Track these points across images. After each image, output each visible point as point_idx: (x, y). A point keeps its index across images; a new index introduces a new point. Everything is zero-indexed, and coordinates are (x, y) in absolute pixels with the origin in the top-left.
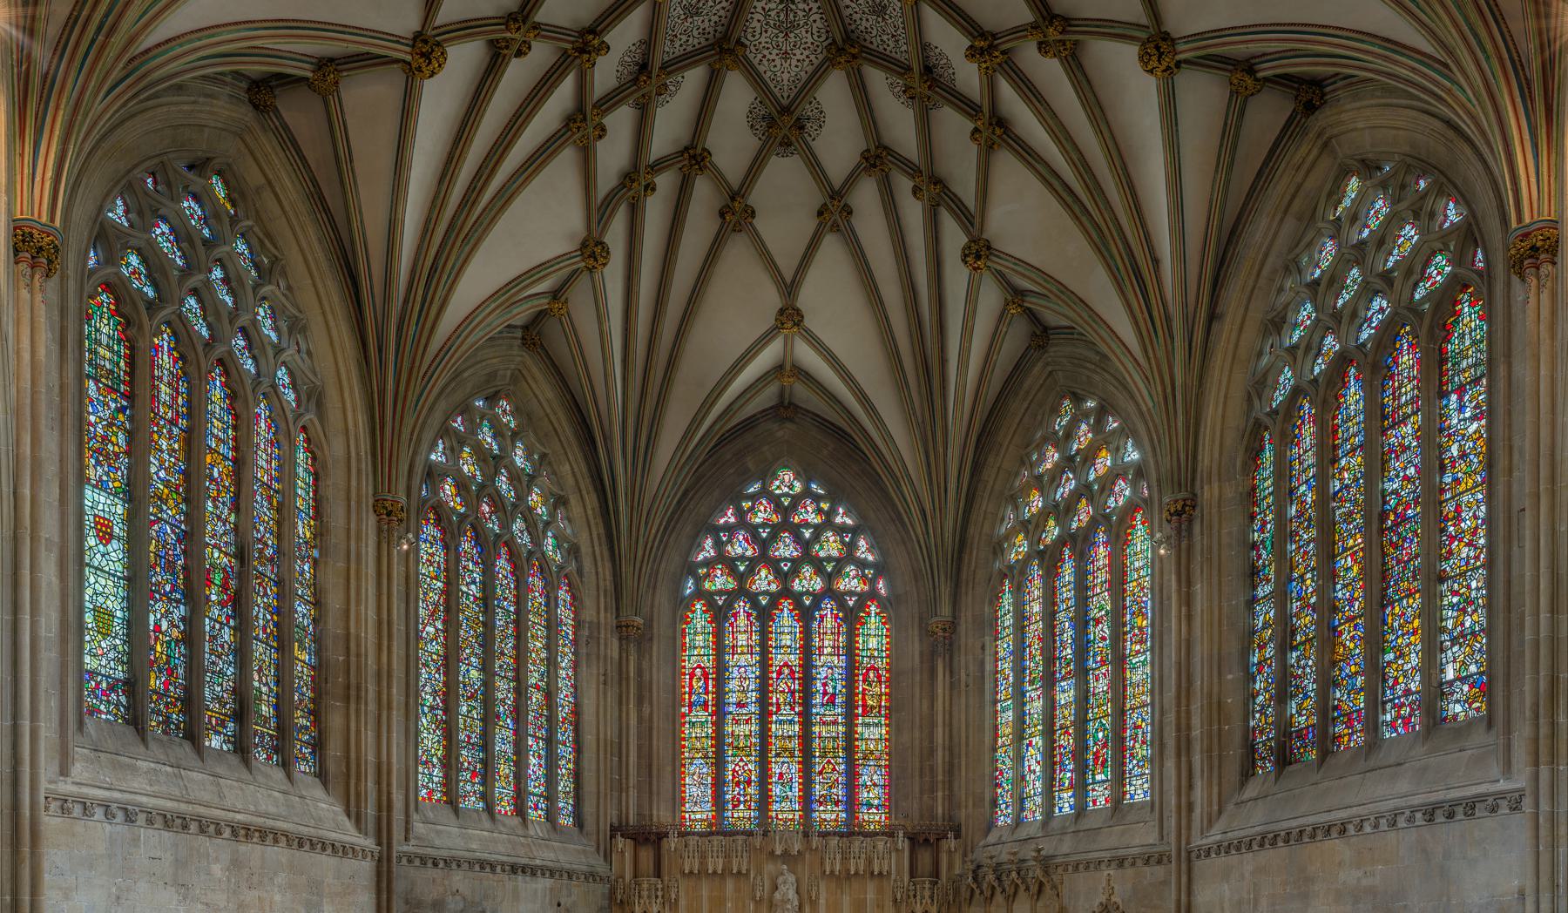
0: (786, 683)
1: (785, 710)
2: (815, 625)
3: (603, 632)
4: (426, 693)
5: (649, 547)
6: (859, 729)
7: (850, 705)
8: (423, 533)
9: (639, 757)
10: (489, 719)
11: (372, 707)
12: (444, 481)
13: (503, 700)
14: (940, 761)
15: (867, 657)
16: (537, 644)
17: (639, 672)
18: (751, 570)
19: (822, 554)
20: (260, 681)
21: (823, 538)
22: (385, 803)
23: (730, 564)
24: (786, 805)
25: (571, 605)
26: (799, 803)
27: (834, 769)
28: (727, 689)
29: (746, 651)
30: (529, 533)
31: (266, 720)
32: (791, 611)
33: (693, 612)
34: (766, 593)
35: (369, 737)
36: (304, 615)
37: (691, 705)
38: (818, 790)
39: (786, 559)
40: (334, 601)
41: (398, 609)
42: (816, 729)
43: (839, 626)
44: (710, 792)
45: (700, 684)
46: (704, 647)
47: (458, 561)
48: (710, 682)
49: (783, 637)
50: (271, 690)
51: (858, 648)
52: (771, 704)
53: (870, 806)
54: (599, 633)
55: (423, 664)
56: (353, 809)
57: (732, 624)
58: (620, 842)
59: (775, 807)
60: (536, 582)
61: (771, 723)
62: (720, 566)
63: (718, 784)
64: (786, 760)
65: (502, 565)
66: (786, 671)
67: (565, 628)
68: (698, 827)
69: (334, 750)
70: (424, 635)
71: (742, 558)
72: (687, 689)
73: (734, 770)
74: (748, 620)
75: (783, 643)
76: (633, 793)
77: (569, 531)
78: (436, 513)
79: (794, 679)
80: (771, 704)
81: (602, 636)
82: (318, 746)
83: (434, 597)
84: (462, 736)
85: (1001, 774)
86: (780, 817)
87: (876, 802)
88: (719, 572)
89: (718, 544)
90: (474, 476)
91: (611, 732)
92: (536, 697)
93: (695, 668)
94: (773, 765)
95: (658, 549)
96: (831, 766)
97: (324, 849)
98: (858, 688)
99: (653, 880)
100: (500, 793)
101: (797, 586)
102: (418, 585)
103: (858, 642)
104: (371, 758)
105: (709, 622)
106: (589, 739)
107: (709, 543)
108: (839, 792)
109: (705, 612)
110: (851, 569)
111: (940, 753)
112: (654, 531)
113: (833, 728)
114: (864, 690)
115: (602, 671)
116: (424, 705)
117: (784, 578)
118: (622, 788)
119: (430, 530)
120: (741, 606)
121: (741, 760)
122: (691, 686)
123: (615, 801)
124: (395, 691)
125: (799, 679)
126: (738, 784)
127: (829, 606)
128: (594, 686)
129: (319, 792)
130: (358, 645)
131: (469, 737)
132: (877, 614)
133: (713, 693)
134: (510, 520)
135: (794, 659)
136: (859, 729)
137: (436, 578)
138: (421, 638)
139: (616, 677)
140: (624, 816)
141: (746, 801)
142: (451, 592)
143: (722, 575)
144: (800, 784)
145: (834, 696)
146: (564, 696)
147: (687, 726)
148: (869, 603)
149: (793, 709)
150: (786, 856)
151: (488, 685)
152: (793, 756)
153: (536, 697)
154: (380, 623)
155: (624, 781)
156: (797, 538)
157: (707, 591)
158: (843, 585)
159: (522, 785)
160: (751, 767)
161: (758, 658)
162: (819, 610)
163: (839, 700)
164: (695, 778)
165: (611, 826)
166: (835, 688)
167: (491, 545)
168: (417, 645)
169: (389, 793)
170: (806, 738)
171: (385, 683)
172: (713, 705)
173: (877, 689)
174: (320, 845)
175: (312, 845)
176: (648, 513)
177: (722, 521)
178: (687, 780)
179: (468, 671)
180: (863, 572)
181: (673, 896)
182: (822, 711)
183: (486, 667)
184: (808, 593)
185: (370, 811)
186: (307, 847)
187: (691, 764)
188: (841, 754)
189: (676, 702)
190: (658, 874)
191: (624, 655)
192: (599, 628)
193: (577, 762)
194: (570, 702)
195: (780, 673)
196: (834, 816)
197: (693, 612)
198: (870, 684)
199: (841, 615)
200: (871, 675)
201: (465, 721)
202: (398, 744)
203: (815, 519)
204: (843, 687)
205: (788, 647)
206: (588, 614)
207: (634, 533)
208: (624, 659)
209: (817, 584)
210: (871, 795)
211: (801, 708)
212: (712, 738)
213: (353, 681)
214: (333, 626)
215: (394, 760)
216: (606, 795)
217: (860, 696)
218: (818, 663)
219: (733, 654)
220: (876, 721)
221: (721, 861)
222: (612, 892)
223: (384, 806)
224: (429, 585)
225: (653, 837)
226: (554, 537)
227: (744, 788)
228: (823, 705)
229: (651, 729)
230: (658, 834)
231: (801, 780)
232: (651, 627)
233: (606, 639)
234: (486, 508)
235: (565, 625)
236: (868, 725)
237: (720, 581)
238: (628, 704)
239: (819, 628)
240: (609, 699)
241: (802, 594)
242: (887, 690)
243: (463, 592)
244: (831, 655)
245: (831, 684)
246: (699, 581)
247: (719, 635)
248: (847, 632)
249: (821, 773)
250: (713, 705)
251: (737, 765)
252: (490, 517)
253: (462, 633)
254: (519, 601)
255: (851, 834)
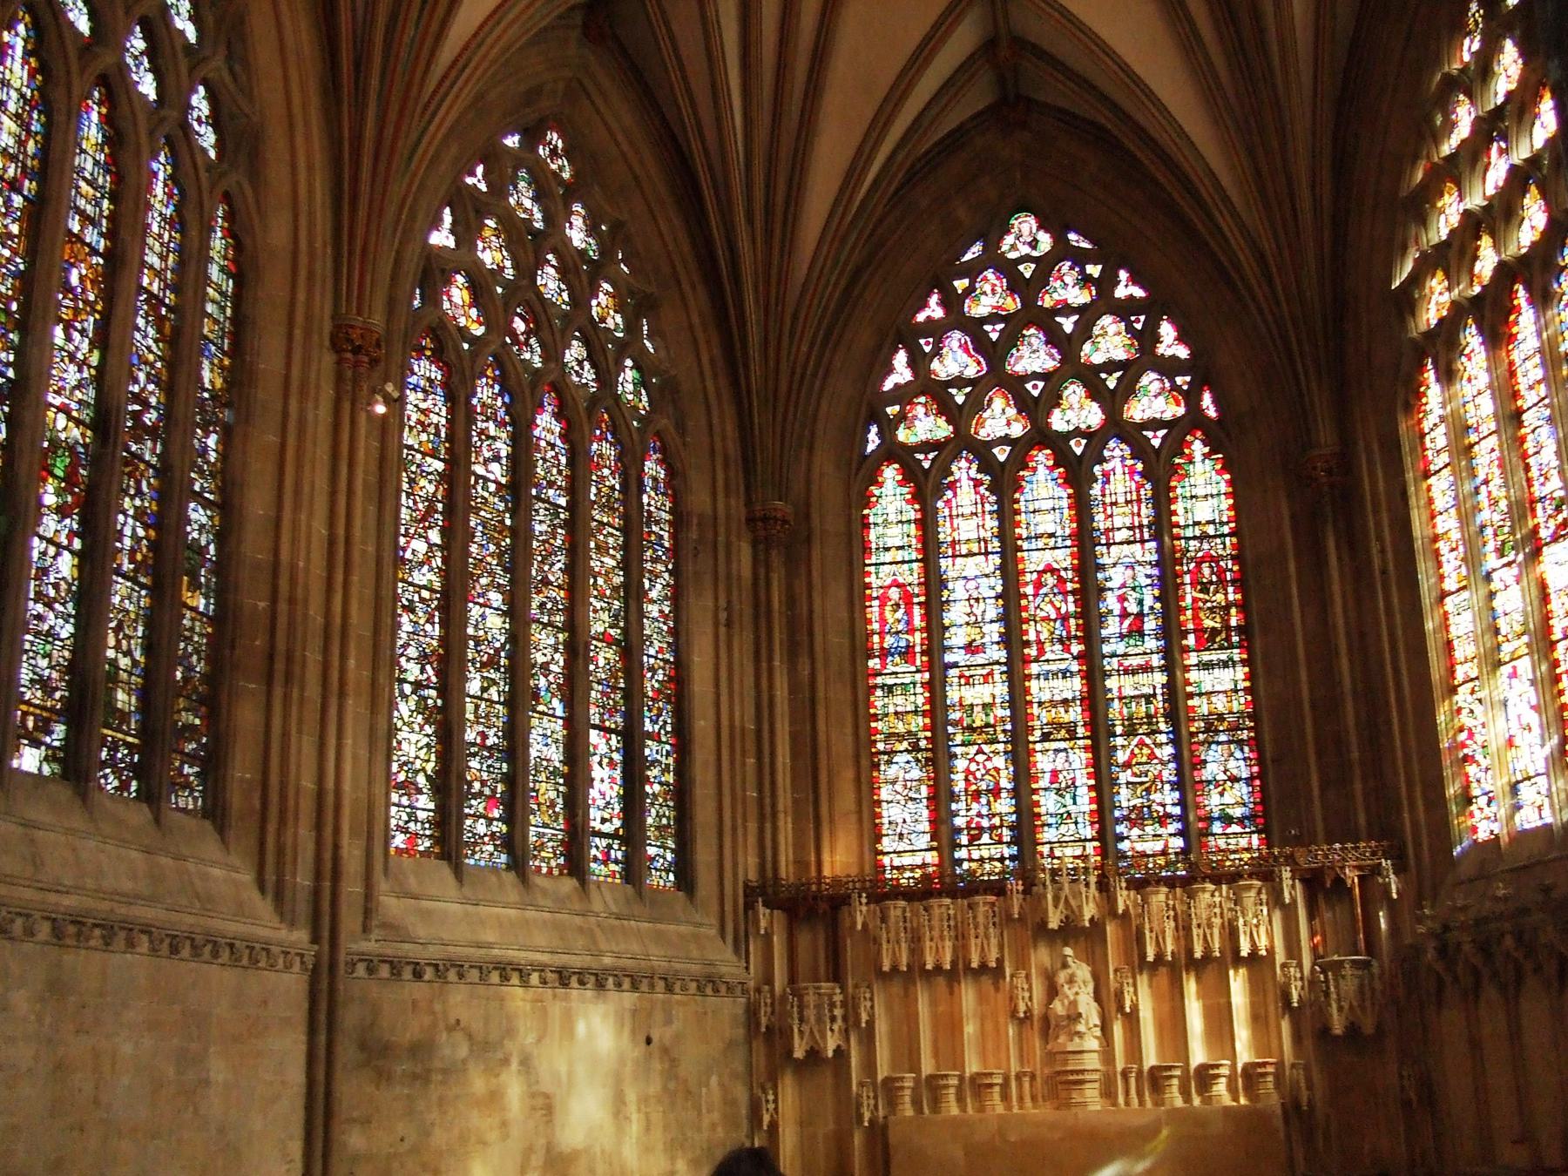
0: (1051, 602)
1: (1053, 651)
2: (1096, 490)
3: (722, 530)
4: (409, 659)
5: (797, 377)
6: (1193, 676)
7: (1170, 632)
8: (413, 373)
9: (795, 755)
10: (519, 701)
11: (313, 690)
12: (449, 282)
13: (545, 667)
14: (1351, 720)
15: (1194, 538)
16: (605, 563)
17: (791, 600)
18: (977, 404)
19: (1098, 359)
20: (117, 647)
21: (1096, 330)
22: (328, 865)
23: (937, 393)
24: (1068, 829)
25: (668, 484)
26: (1092, 823)
27: (1152, 756)
28: (946, 622)
29: (976, 550)
30: (593, 366)
31: (124, 716)
32: (1051, 469)
33: (881, 485)
34: (1005, 440)
35: (306, 747)
36: (202, 526)
37: (885, 654)
38: (1125, 798)
39: (1035, 376)
40: (257, 504)
41: (364, 515)
42: (1111, 683)
43: (1139, 487)
44: (926, 813)
45: (900, 614)
46: (902, 548)
47: (471, 420)
48: (917, 611)
49: (1038, 518)
50: (135, 663)
51: (1177, 525)
52: (1027, 644)
53: (1227, 820)
54: (716, 534)
55: (403, 606)
56: (271, 878)
57: (948, 502)
58: (763, 911)
59: (1049, 835)
60: (604, 449)
61: (1029, 677)
62: (922, 399)
63: (940, 798)
64: (1062, 745)
65: (546, 425)
66: (1050, 580)
67: (655, 528)
68: (906, 879)
69: (242, 770)
70: (408, 555)
71: (959, 382)
72: (876, 626)
73: (968, 771)
74: (977, 493)
75: (1040, 530)
76: (786, 825)
77: (663, 354)
78: (436, 339)
79: (1065, 593)
80: (1027, 644)
81: (721, 539)
82: (213, 764)
83: (427, 487)
84: (470, 735)
85: (1471, 735)
86: (1057, 853)
87: (1237, 812)
88: (920, 410)
89: (918, 362)
90: (502, 269)
91: (745, 715)
92: (604, 657)
93: (889, 587)
94: (1039, 755)
95: (814, 375)
96: (1146, 751)
97: (215, 954)
98: (1183, 598)
99: (825, 987)
100: (540, 835)
101: (1059, 422)
102: (403, 465)
103: (1174, 513)
104: (308, 784)
105: (908, 502)
106: (702, 725)
107: (901, 359)
108: (1167, 798)
109: (901, 484)
110: (1150, 380)
111: (1349, 707)
112: (804, 349)
113: (1142, 678)
114: (1195, 600)
115: (722, 603)
116: (405, 681)
117: (1035, 409)
118: (767, 814)
119: (424, 369)
120: (964, 470)
121: (980, 751)
122: (883, 621)
123: (752, 839)
124: (352, 663)
125: (1073, 592)
126: (976, 795)
127: (1117, 453)
128: (709, 630)
129: (210, 846)
130: (293, 581)
131: (484, 736)
132: (1206, 456)
133: (921, 630)
134: (559, 345)
135: (1063, 558)
136: (1193, 676)
137: (434, 454)
138: (403, 560)
139: (748, 611)
140: (769, 866)
141: (993, 828)
142: (456, 477)
143: (926, 414)
144: (1091, 788)
145: (1140, 616)
146: (656, 650)
147: (879, 693)
148: (1189, 438)
149: (1067, 649)
150: (1070, 931)
151: (518, 639)
152: (1072, 736)
153: (604, 657)
154: (332, 542)
155: (768, 801)
156: (1054, 337)
157: (903, 446)
158: (1137, 411)
159: (579, 819)
160: (999, 761)
161: (998, 561)
162: (1100, 463)
163: (1150, 624)
164: (899, 787)
165: (746, 886)
166: (1140, 602)
167: (527, 392)
168: (396, 574)
169: (337, 847)
170: (1094, 700)
171: (336, 650)
172: (923, 653)
173: (1220, 597)
174: (209, 947)
175: (193, 947)
176: (795, 317)
177: (921, 317)
178: (885, 793)
179: (483, 616)
180: (1173, 382)
181: (864, 1017)
182: (1120, 648)
183: (515, 611)
184: (1077, 432)
185: (303, 879)
186: (186, 952)
187: (889, 762)
188: (1162, 726)
189: (859, 647)
190: (837, 976)
191: (762, 571)
192: (715, 526)
193: (682, 769)
194: (666, 661)
195: (1038, 585)
196: (1159, 846)
197: (881, 485)
198: (1205, 590)
199: (1140, 467)
200: (1206, 571)
201: (477, 707)
202: (355, 757)
203: (1079, 296)
204: (1157, 599)
205: (1052, 535)
206: (699, 500)
207: (772, 354)
208: (762, 576)
209: (1093, 416)
210: (1228, 799)
211: (1082, 647)
212: (925, 714)
213: (281, 645)
214: (253, 546)
215: (347, 787)
216: (734, 829)
217: (1189, 613)
218: (1105, 560)
219: (954, 556)
220: (1224, 657)
221: (948, 944)
222: (752, 1012)
223: (329, 870)
224: (419, 466)
225: (823, 907)
226: (636, 367)
227: (989, 803)
228: (1122, 637)
229: (813, 701)
230: (831, 898)
231: (1092, 782)
232: (808, 517)
233: (728, 545)
234: (519, 325)
235: (657, 523)
236: (1207, 666)
237: (926, 426)
238: (770, 659)
239: (1103, 495)
240: (736, 655)
241: (1068, 436)
242: (1239, 596)
243: (478, 477)
244: (1129, 543)
245: (1133, 596)
246: (888, 428)
247: (927, 525)
248: (1153, 497)
249: (1127, 765)
250: (923, 653)
251: (972, 760)
252: (527, 340)
253: (474, 548)
254: (575, 488)
255: (1191, 880)
